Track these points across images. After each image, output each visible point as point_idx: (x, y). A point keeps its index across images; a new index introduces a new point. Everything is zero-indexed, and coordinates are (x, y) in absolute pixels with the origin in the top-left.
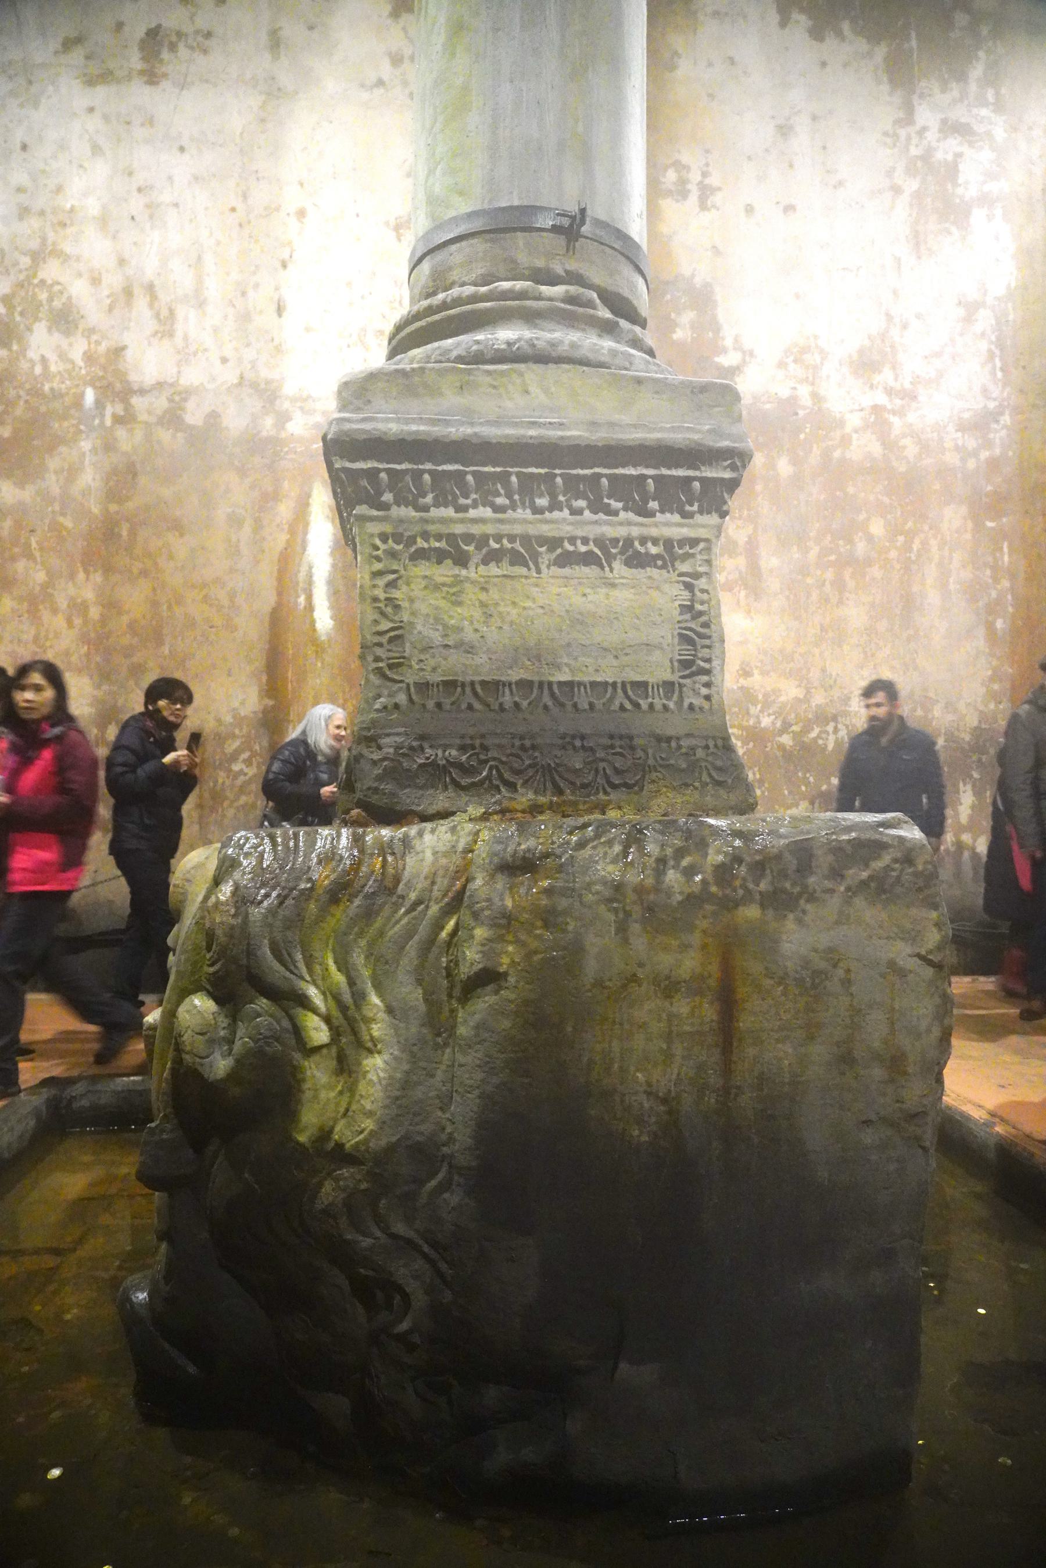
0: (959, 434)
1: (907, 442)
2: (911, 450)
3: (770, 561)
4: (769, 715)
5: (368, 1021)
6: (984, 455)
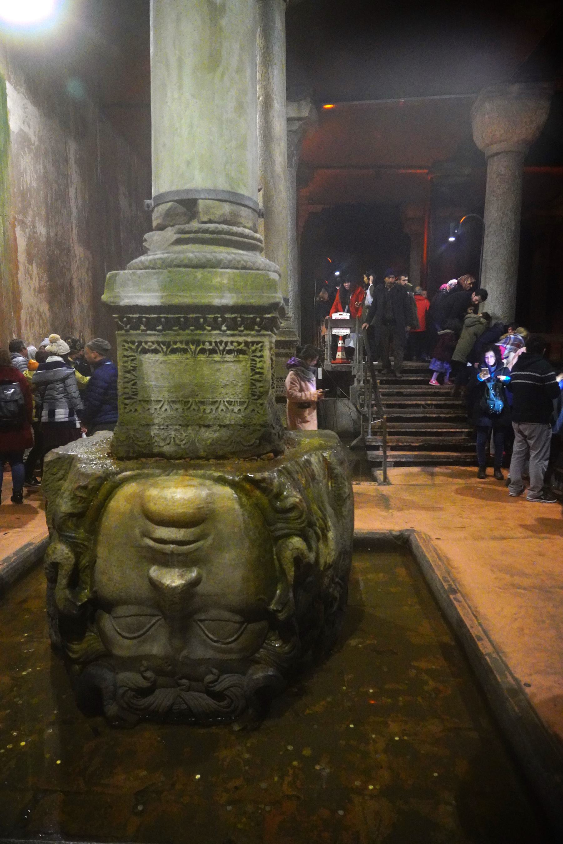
5: (328, 523)
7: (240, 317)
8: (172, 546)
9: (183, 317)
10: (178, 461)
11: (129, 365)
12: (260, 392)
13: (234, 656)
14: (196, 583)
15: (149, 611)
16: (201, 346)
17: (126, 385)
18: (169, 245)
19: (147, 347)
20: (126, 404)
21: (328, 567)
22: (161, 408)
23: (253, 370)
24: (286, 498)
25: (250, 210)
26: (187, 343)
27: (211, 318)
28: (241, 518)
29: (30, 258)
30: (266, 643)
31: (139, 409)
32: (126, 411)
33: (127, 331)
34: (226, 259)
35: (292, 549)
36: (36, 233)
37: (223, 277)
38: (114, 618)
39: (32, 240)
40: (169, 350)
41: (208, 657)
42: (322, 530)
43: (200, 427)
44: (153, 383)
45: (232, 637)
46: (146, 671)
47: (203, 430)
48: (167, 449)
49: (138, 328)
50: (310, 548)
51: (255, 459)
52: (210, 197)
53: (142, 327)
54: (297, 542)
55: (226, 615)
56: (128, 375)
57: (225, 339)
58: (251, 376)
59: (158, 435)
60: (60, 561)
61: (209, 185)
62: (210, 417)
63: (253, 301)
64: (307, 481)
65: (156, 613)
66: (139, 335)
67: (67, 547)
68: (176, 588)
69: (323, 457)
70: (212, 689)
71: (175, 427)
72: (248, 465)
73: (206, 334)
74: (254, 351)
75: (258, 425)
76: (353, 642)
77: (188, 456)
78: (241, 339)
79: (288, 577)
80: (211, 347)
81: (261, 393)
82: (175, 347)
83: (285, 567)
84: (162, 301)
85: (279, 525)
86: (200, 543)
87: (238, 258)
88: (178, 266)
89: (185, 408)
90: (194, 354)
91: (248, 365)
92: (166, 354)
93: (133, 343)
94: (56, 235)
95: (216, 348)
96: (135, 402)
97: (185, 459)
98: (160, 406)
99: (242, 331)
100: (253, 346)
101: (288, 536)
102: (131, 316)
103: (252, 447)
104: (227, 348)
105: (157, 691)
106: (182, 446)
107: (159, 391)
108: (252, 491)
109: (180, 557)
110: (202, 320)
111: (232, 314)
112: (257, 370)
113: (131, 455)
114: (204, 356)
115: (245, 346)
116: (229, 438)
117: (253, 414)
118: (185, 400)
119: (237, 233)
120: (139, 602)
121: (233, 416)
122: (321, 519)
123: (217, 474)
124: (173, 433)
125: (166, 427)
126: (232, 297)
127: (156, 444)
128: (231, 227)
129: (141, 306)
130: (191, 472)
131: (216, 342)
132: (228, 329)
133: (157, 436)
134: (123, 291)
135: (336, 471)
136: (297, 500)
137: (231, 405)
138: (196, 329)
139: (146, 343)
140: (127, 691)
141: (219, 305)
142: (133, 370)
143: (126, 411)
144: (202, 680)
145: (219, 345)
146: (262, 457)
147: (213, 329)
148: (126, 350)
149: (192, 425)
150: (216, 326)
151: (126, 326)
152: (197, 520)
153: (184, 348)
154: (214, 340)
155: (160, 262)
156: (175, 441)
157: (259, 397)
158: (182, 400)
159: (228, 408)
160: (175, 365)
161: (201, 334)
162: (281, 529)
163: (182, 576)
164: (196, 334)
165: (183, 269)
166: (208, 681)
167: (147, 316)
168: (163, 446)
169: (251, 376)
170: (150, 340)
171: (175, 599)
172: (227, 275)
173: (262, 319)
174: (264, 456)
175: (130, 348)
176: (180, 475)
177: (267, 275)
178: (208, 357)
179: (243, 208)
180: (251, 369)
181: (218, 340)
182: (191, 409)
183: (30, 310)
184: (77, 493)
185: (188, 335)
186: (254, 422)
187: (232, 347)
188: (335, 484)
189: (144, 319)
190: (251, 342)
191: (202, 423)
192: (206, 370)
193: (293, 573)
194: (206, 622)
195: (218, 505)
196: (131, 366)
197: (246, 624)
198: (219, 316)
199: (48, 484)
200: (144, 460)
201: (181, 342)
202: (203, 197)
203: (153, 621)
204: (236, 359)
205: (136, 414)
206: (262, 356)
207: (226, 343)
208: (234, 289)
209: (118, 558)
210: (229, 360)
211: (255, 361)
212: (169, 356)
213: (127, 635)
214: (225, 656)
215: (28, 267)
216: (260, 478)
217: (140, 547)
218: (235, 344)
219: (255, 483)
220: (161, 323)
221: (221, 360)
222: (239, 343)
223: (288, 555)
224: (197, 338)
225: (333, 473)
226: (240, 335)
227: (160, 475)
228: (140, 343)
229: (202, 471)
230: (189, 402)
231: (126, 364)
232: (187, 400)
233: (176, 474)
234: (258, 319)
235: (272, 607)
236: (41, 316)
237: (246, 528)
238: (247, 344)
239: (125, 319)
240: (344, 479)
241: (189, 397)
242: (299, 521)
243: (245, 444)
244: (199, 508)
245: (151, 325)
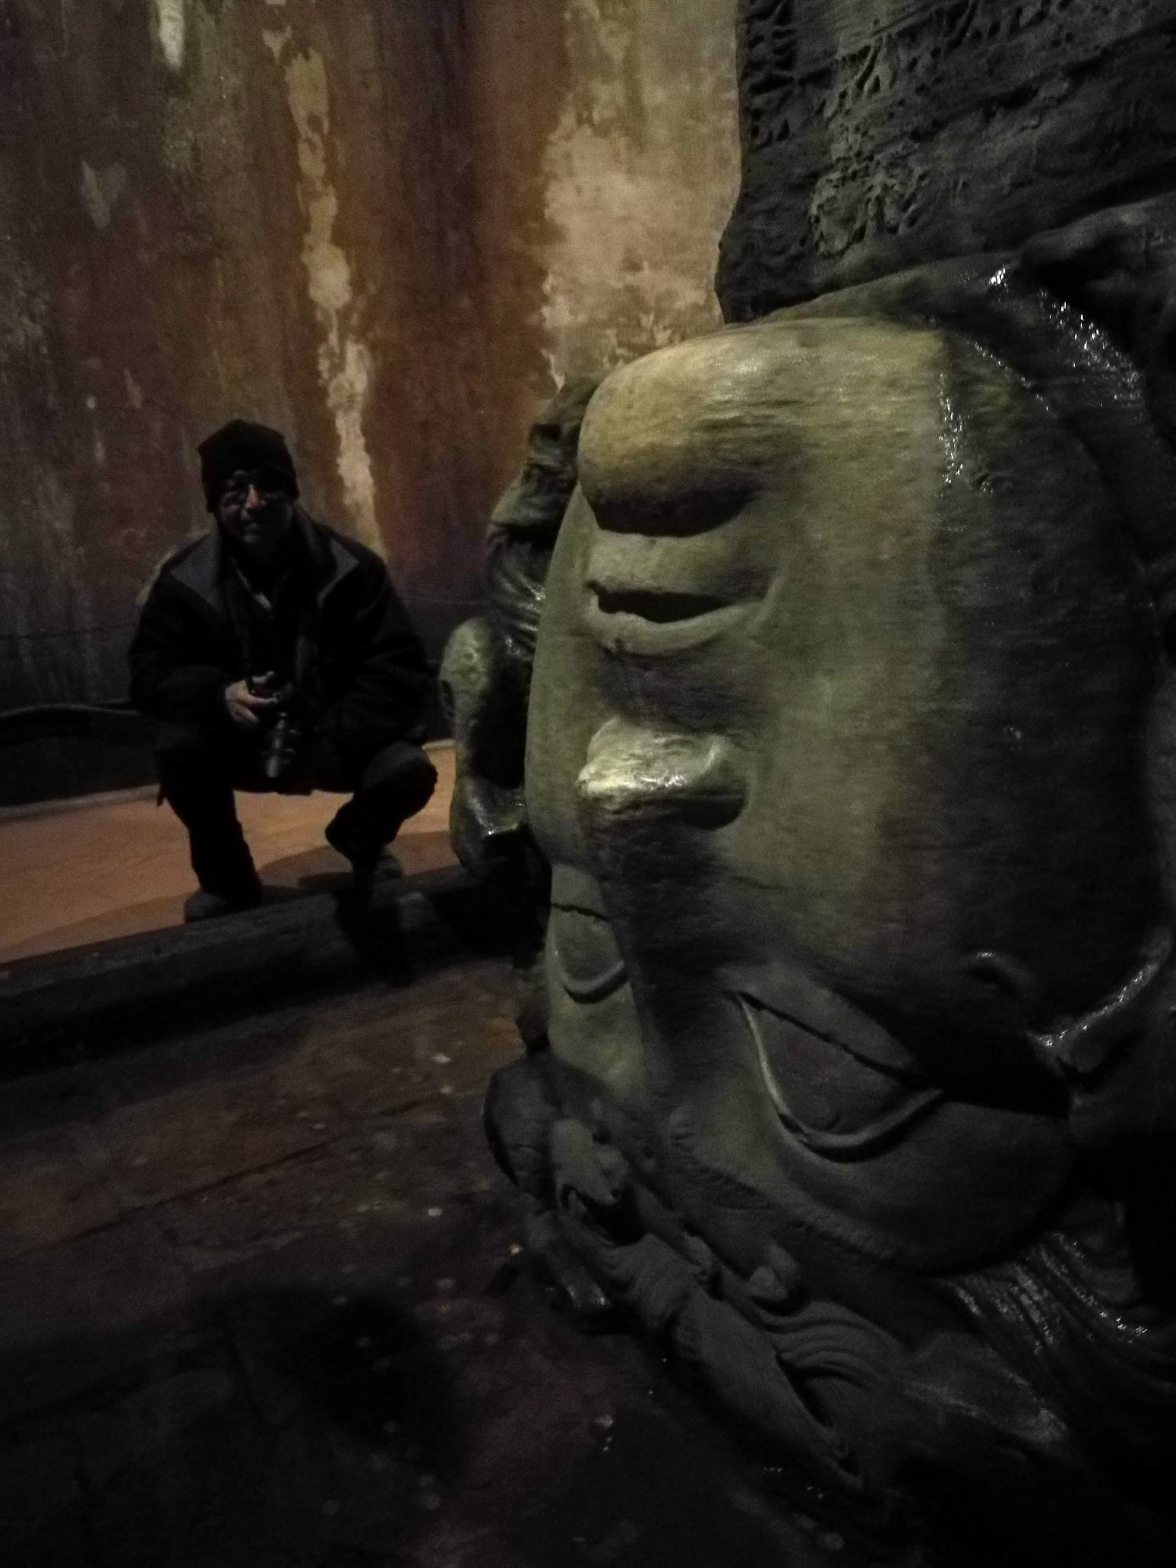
3: (655, 95)
4: (665, 328)
13: (854, 1233)
41: (751, 1182)
45: (848, 1130)
55: (821, 1004)
106: (902, 230)
127: (822, 248)
166: (756, 1291)
194: (765, 1013)
214: (820, 1210)
244: (714, 426)
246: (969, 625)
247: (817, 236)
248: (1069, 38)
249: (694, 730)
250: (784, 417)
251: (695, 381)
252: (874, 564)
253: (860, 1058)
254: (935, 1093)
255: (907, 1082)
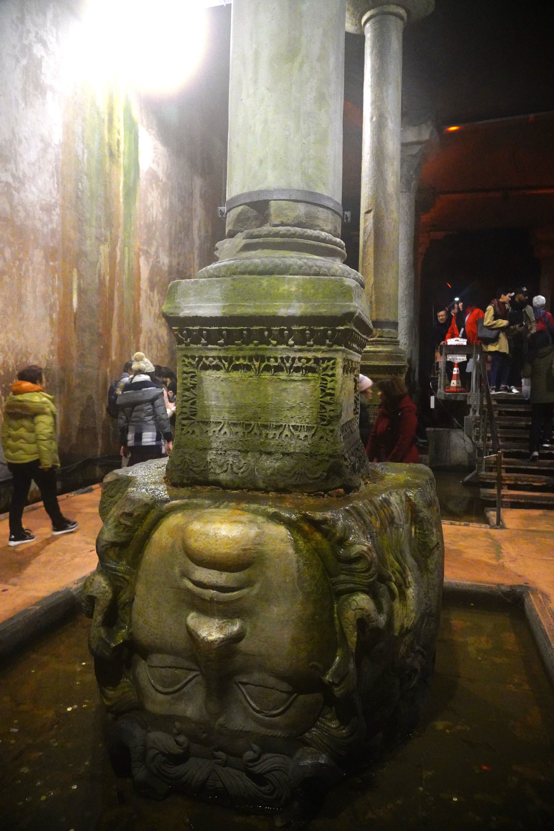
0: (40, 212)
1: (20, 208)
2: (22, 214)
5: (407, 576)
6: (50, 226)
7: (308, 330)
8: (212, 592)
9: (246, 330)
10: (235, 492)
11: (189, 382)
12: (330, 416)
13: (279, 733)
14: (238, 637)
15: (187, 664)
16: (266, 363)
17: (185, 404)
18: (237, 252)
19: (208, 363)
20: (184, 425)
21: (405, 632)
22: (220, 430)
23: (323, 391)
24: (353, 544)
25: (329, 212)
26: (251, 359)
27: (276, 330)
28: (295, 565)
29: (152, 285)
30: (319, 721)
31: (197, 431)
32: (184, 432)
33: (188, 345)
34: (296, 264)
35: (356, 609)
36: (159, 262)
37: (291, 285)
38: (149, 666)
39: (155, 270)
40: (231, 366)
42: (399, 586)
43: (261, 454)
44: (213, 403)
45: (277, 709)
46: (178, 734)
47: (264, 457)
48: (223, 477)
49: (198, 342)
50: (379, 608)
51: (321, 495)
52: (283, 198)
53: (203, 341)
54: (362, 601)
55: (272, 681)
56: (187, 393)
57: (292, 355)
58: (321, 398)
59: (215, 461)
60: (96, 595)
61: (283, 184)
62: (273, 442)
63: (323, 311)
64: (382, 524)
65: (194, 667)
66: (199, 349)
67: (105, 580)
68: (212, 642)
69: (407, 496)
70: (251, 769)
71: (233, 453)
72: (311, 501)
73: (271, 349)
74: (325, 369)
75: (327, 455)
76: (440, 725)
77: (245, 486)
78: (310, 355)
79: (349, 643)
80: (277, 364)
81: (331, 417)
82: (238, 363)
83: (346, 630)
84: (224, 311)
85: (342, 577)
86: (245, 591)
87: (310, 263)
88: (243, 273)
89: (246, 431)
90: (259, 371)
91: (318, 385)
92: (228, 371)
93: (193, 358)
94: (178, 264)
95: (282, 365)
96: (193, 423)
97: (242, 489)
98: (219, 428)
99: (312, 346)
100: (323, 363)
101: (352, 592)
102: (191, 328)
103: (319, 480)
104: (295, 365)
105: (192, 760)
106: (240, 475)
107: (218, 412)
108: (312, 534)
109: (221, 606)
110: (266, 333)
111: (300, 326)
112: (328, 391)
113: (185, 481)
114: (269, 374)
115: (314, 363)
116: (293, 468)
117: (322, 441)
118: (246, 422)
119: (311, 236)
120: (174, 652)
121: (298, 443)
122: (399, 572)
123: (271, 510)
124: (231, 459)
125: (224, 452)
126: (300, 307)
128: (305, 230)
129: (200, 317)
130: (243, 505)
131: (282, 358)
132: (296, 344)
133: (213, 462)
134: (183, 301)
135: (421, 515)
136: (365, 548)
137: (297, 430)
138: (261, 343)
139: (207, 358)
140: (158, 754)
141: (285, 316)
142: (193, 388)
143: (184, 432)
144: (241, 757)
145: (285, 361)
146: (330, 492)
147: (279, 343)
148: (187, 366)
149: (253, 451)
150: (282, 340)
151: (186, 340)
152: (244, 563)
153: (247, 364)
154: (280, 356)
155: (225, 269)
156: (232, 469)
157: (329, 423)
158: (243, 423)
159: (293, 433)
160: (237, 384)
161: (266, 349)
162: (343, 582)
163: (221, 628)
164: (260, 349)
165: (247, 276)
167: (208, 328)
168: (219, 474)
169: (321, 398)
170: (211, 355)
171: (211, 655)
172: (296, 282)
173: (334, 331)
174: (332, 492)
175: (189, 363)
176: (231, 508)
177: (342, 281)
178: (273, 375)
179: (321, 209)
180: (321, 390)
181: (284, 356)
182: (253, 433)
183: (149, 334)
184: (122, 520)
185: (252, 349)
186: (322, 451)
187: (300, 364)
188: (419, 529)
189: (204, 332)
190: (321, 359)
191: (263, 449)
192: (270, 390)
193: (355, 639)
194: (248, 686)
195: (267, 548)
196: (191, 384)
197: (295, 694)
198: (285, 328)
199: (105, 507)
200: (198, 488)
201: (244, 358)
202: (275, 197)
203: (190, 677)
204: (304, 378)
205: (194, 436)
206: (333, 375)
207: (294, 359)
208: (304, 298)
209: (155, 599)
210: (296, 378)
211: (326, 380)
212: (231, 373)
213: (160, 688)
214: (269, 731)
215: (150, 295)
216: (321, 519)
217: (179, 588)
218: (304, 361)
219: (316, 525)
220: (223, 337)
221: (289, 378)
222: (308, 360)
223: (350, 615)
224: (260, 353)
225: (418, 516)
226: (309, 351)
227: (209, 507)
228: (201, 358)
229: (256, 506)
230: (250, 425)
231: (185, 382)
232: (248, 422)
233: (226, 507)
234: (330, 332)
235: (328, 678)
236: (159, 341)
237: (300, 578)
238: (317, 360)
239: (185, 332)
240: (431, 525)
241: (251, 419)
242: (366, 574)
243: (310, 476)
244: (244, 550)
245: (212, 338)
246: (307, 595)
247: (210, 467)
248: (282, 446)
249: (231, 618)
250: (259, 547)
251: (237, 538)
252: (285, 582)
253: (281, 691)
254: (295, 694)
255: (290, 694)
